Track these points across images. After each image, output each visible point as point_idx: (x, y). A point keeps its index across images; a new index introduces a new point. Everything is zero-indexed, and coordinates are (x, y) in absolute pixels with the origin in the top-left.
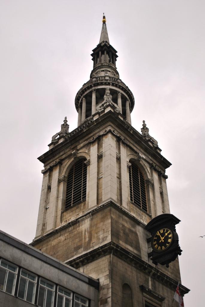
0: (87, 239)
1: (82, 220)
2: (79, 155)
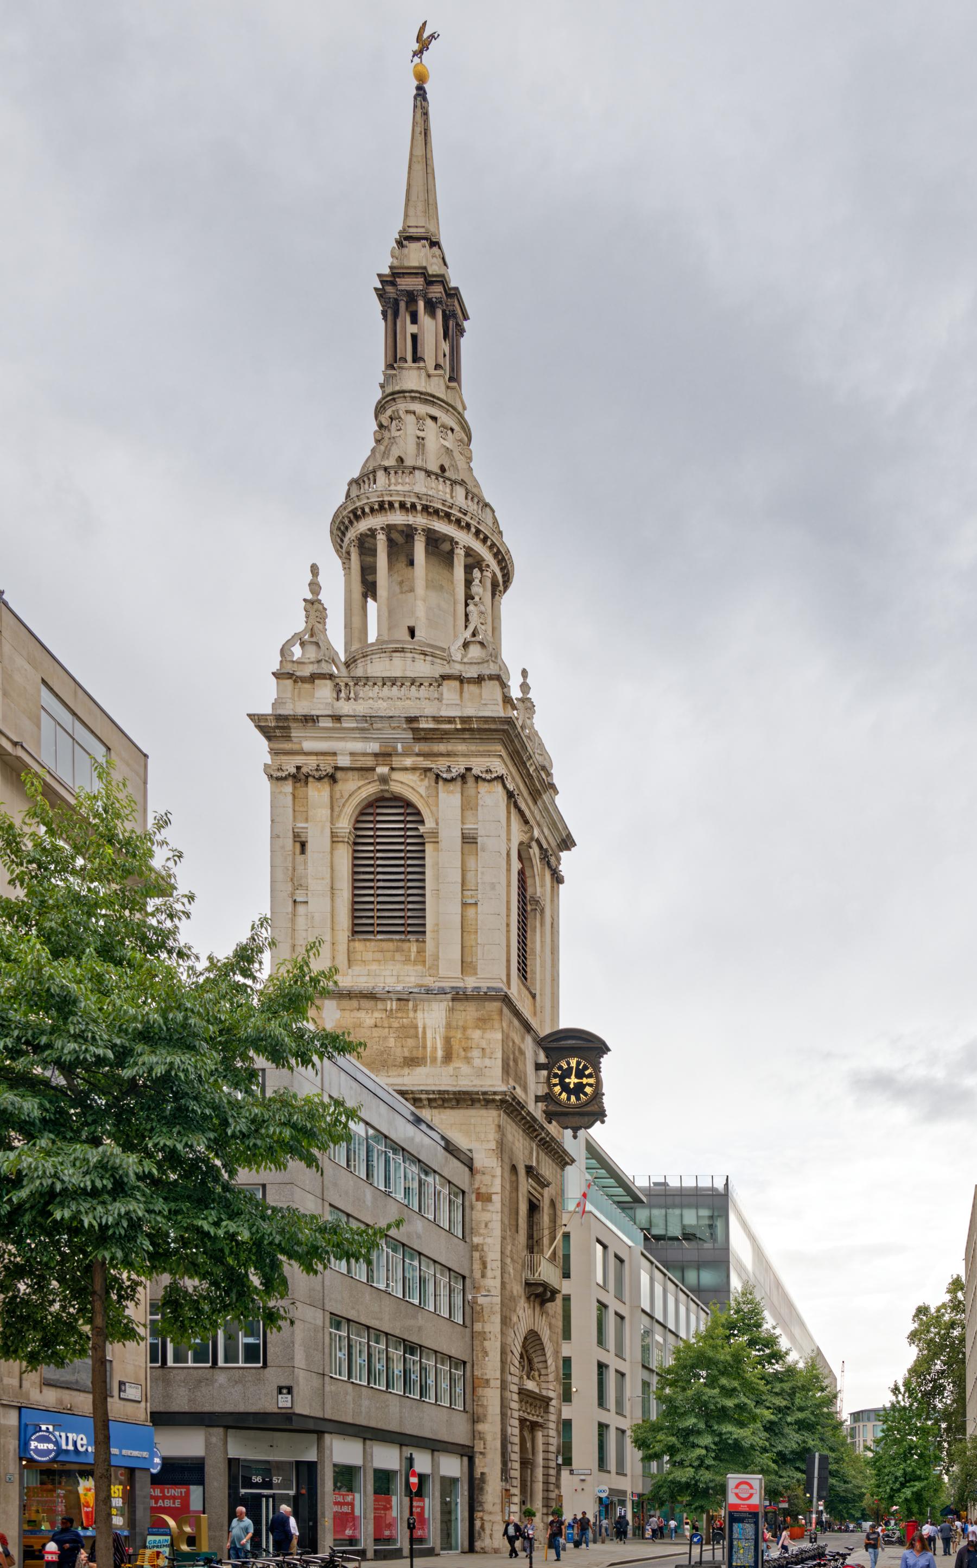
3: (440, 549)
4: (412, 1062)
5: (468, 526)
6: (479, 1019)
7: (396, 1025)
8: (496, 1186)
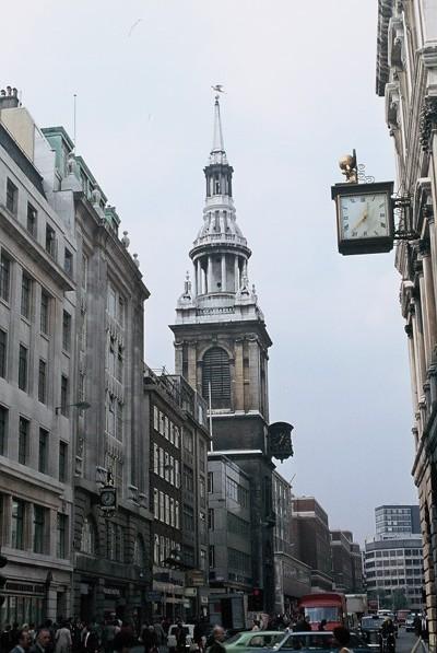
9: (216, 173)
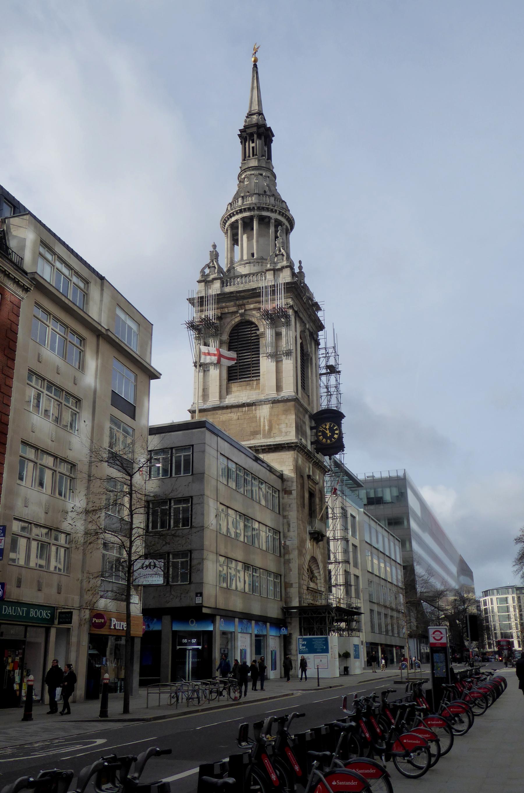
0: (267, 428)
1: (262, 405)
2: (247, 318)
3: (264, 221)
4: (255, 433)
5: (276, 211)
6: (285, 410)
7: (247, 417)
8: (294, 487)
9: (251, 135)
